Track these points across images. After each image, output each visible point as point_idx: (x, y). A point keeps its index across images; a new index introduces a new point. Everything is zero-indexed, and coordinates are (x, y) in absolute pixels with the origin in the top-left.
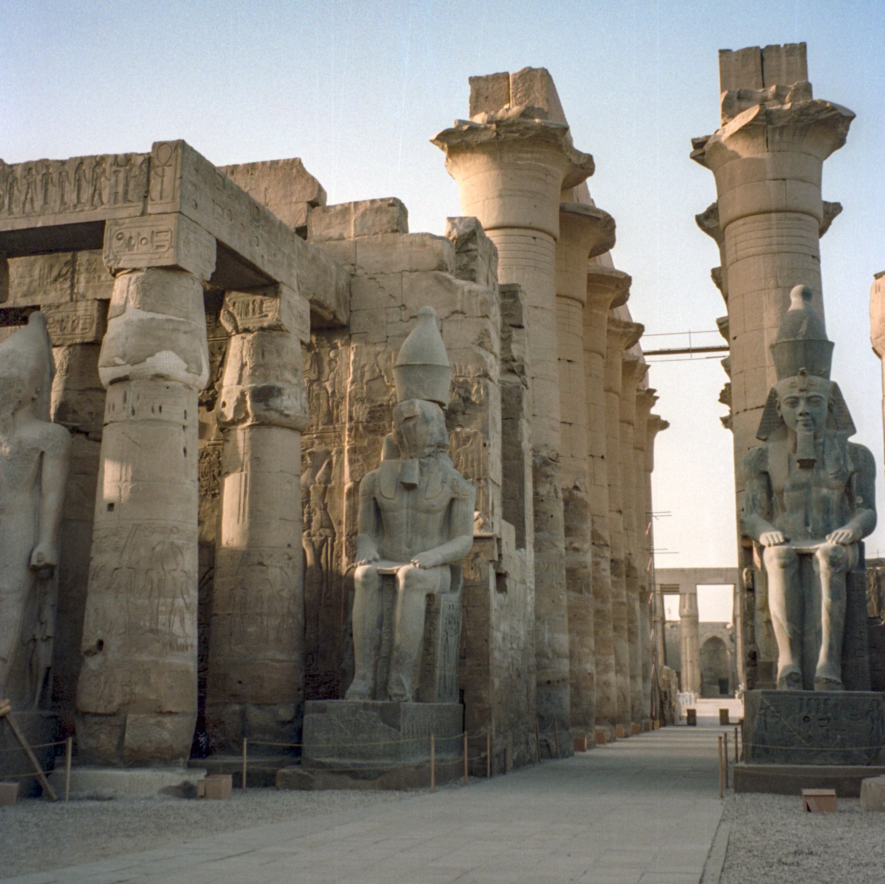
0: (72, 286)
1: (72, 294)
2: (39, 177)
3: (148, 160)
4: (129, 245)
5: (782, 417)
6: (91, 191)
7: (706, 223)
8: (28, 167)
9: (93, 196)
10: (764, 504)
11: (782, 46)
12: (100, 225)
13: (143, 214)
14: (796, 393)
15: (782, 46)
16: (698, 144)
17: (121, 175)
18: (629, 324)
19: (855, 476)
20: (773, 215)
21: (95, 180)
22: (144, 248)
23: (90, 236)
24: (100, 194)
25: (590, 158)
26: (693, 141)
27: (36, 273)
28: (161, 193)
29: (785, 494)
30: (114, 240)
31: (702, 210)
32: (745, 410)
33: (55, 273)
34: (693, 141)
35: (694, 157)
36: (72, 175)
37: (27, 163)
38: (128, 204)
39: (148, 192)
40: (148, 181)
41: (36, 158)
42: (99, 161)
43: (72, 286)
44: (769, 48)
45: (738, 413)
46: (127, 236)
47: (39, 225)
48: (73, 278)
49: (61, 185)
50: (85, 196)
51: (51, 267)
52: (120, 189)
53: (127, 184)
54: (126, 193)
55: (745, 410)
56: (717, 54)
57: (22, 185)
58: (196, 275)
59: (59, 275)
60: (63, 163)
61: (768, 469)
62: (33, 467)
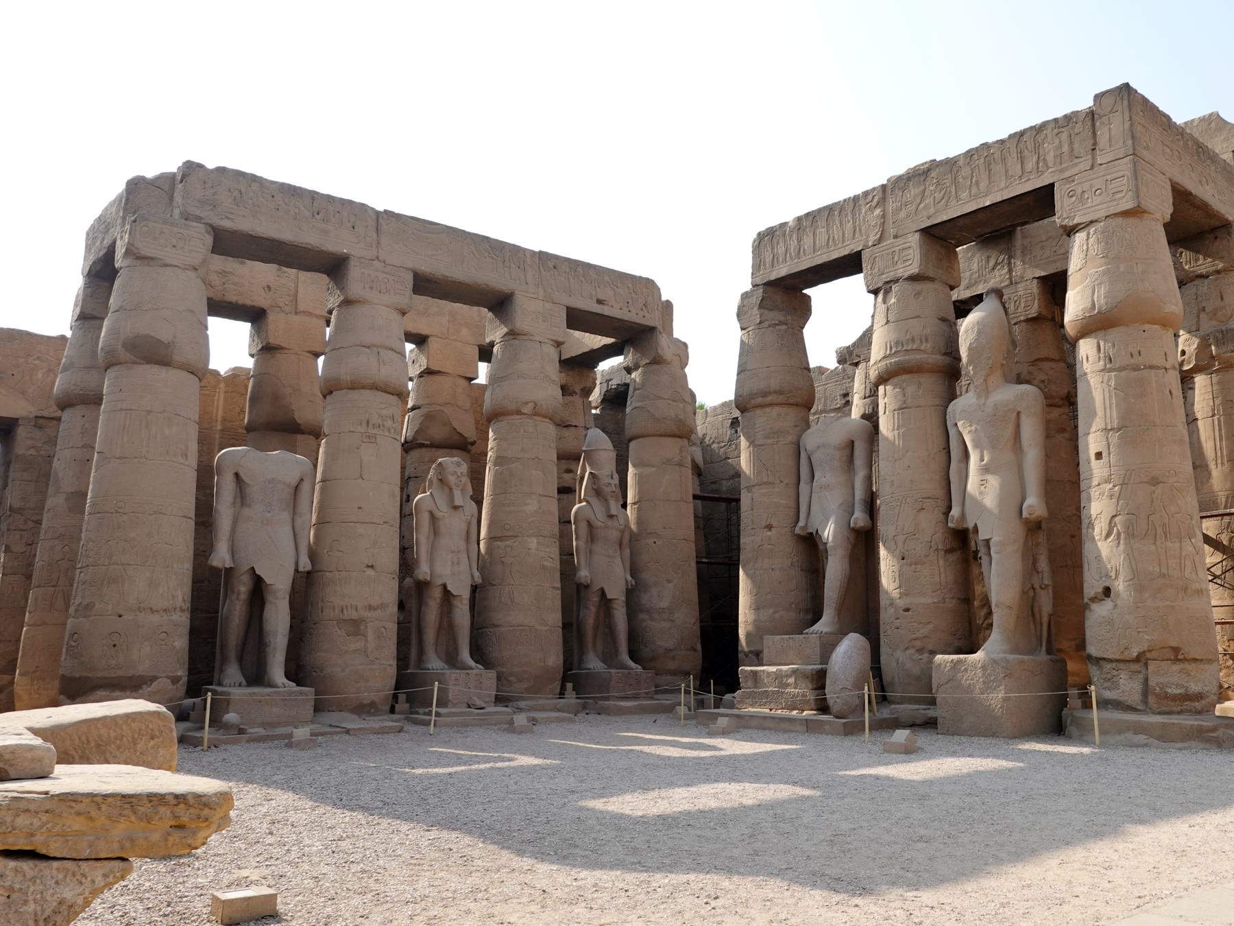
0: (1010, 271)
1: (1010, 278)
2: (982, 160)
3: (1091, 114)
4: (1082, 200)
6: (1035, 159)
8: (970, 154)
9: (1038, 163)
12: (1049, 190)
13: (1092, 167)
17: (1064, 136)
21: (1037, 147)
22: (1098, 200)
23: (1041, 202)
24: (1044, 160)
27: (975, 267)
28: (1110, 140)
30: (1066, 199)
33: (992, 263)
36: (1013, 150)
37: (968, 152)
38: (1076, 161)
39: (1095, 144)
40: (1094, 133)
41: (976, 144)
42: (1039, 129)
43: (1010, 271)
46: (1079, 191)
47: (988, 203)
48: (1010, 263)
49: (1004, 159)
50: (1030, 165)
51: (988, 258)
52: (1065, 148)
53: (1071, 143)
54: (1072, 150)
57: (965, 171)
58: (1158, 216)
59: (996, 264)
60: (1002, 142)
62: (1010, 428)
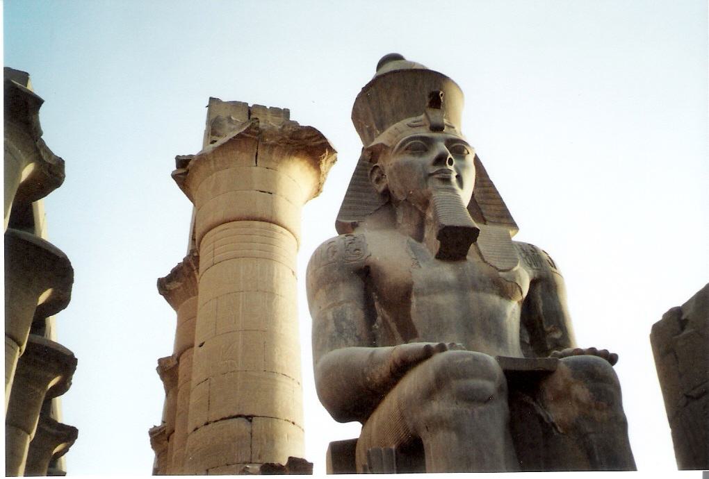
5: (387, 193)
7: (168, 286)
10: (360, 328)
11: (268, 107)
14: (424, 132)
15: (268, 107)
16: (183, 162)
18: (62, 426)
19: (539, 289)
20: (257, 223)
25: (60, 163)
26: (178, 158)
29: (414, 300)
31: (165, 272)
32: (207, 424)
34: (178, 158)
35: (175, 176)
44: (256, 106)
45: (196, 429)
55: (207, 424)
56: (208, 100)
61: (371, 259)
